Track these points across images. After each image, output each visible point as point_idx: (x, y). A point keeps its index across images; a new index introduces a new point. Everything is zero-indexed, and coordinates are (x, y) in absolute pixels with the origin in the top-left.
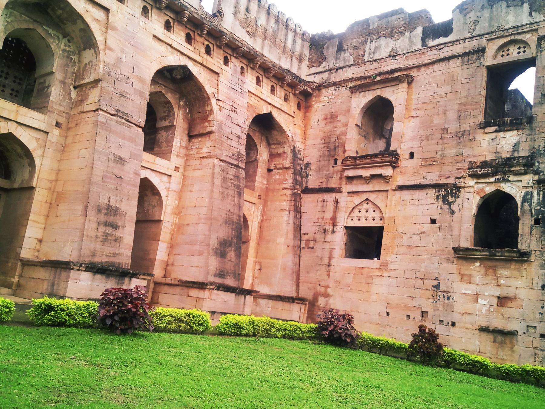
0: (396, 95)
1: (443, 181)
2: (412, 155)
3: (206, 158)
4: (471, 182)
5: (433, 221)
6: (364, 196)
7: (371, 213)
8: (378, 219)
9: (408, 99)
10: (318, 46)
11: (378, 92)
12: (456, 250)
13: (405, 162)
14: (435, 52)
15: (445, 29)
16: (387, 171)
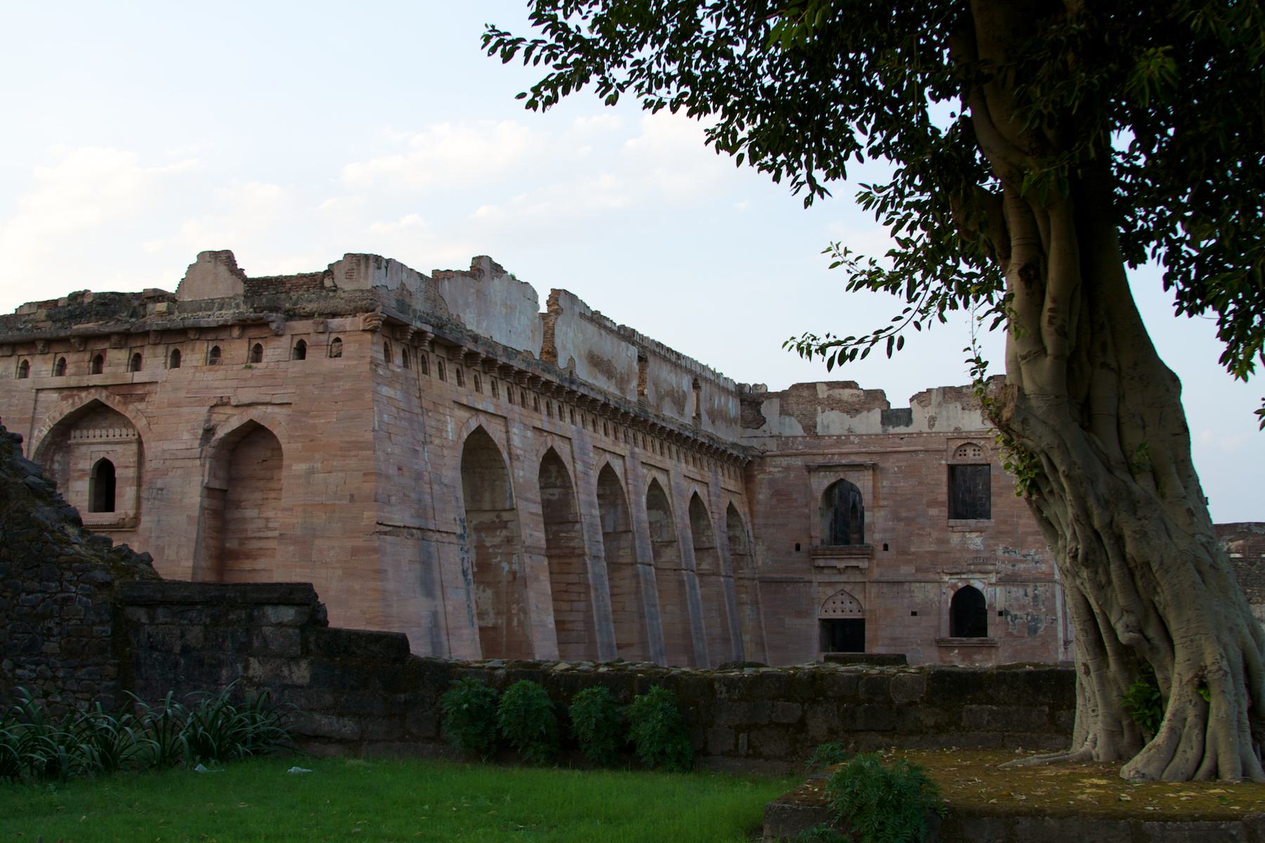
0: (862, 482)
1: (920, 576)
2: (886, 547)
3: (709, 575)
4: (946, 578)
5: (914, 614)
6: (839, 587)
7: (848, 606)
8: (855, 611)
9: (874, 487)
10: (751, 400)
11: (842, 476)
12: (937, 642)
13: (880, 554)
14: (897, 440)
15: (904, 416)
16: (863, 564)
